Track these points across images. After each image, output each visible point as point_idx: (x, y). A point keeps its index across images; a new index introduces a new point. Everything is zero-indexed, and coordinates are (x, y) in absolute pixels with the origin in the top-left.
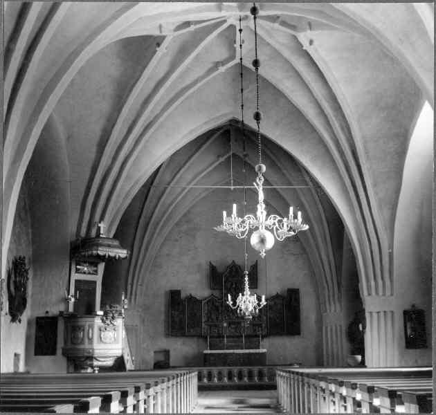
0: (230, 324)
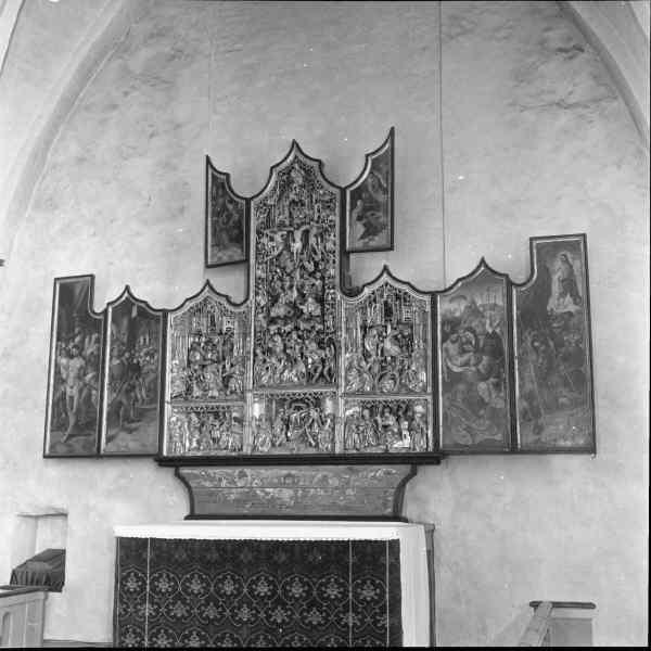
0: (270, 401)
